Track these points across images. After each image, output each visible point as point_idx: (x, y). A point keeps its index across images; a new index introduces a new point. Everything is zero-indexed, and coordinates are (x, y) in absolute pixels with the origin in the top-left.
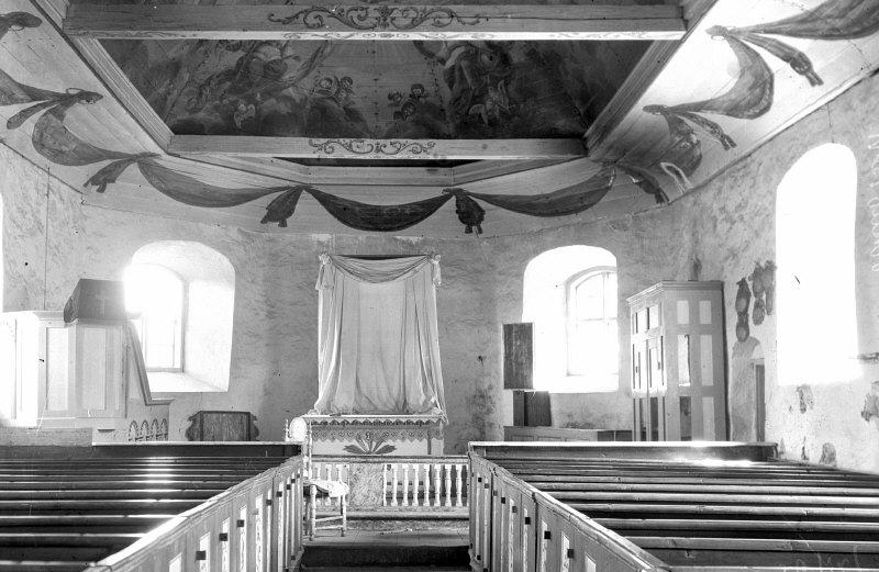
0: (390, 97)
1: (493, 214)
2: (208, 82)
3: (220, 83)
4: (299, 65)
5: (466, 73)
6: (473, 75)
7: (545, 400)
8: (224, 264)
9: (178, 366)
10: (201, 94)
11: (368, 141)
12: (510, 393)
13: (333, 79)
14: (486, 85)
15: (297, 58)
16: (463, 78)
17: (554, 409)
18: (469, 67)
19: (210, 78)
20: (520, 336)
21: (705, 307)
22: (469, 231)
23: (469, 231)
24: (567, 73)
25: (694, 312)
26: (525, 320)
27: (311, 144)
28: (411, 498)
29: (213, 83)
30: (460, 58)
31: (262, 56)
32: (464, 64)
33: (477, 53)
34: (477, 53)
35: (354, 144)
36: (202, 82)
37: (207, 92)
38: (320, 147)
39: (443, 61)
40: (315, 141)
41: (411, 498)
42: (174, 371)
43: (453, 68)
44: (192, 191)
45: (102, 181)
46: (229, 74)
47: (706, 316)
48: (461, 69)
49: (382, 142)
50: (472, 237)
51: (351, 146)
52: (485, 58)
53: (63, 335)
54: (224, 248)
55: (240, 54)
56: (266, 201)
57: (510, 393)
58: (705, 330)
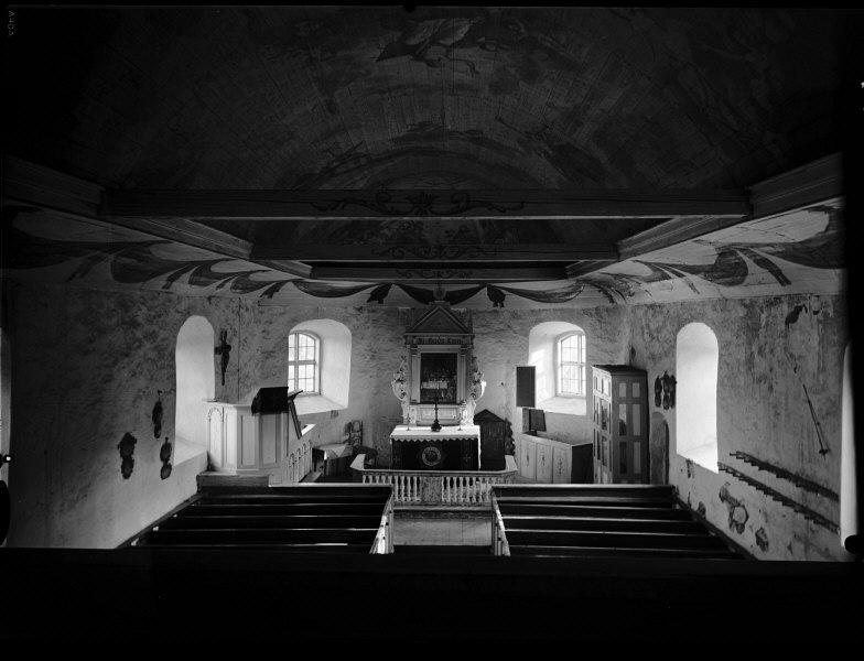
0: (447, 232)
1: (510, 299)
7: (542, 413)
8: (344, 330)
9: (317, 391)
11: (432, 270)
12: (521, 409)
17: (548, 422)
20: (526, 377)
21: (636, 387)
22: (496, 305)
23: (496, 305)
25: (629, 391)
26: (531, 363)
28: (458, 481)
38: (403, 275)
40: (401, 270)
41: (458, 481)
42: (315, 395)
44: (325, 290)
45: (270, 293)
47: (636, 392)
50: (498, 308)
53: (252, 421)
54: (344, 321)
56: (370, 290)
57: (521, 409)
58: (636, 401)
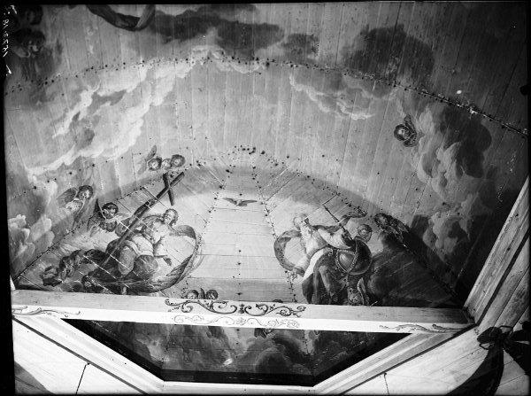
2: (74, 255)
3: (86, 261)
4: (170, 269)
5: (324, 279)
6: (331, 280)
10: (62, 266)
13: (199, 292)
14: (346, 288)
15: (168, 260)
16: (321, 284)
18: (328, 271)
19: (76, 252)
24: (434, 237)
27: (167, 302)
29: (79, 259)
30: (318, 265)
31: (134, 246)
32: (323, 269)
33: (334, 255)
34: (334, 255)
35: (216, 306)
36: (67, 254)
37: (69, 267)
39: (302, 272)
43: (311, 277)
46: (98, 255)
48: (319, 277)
49: (247, 304)
51: (212, 306)
52: (343, 257)
55: (113, 236)
